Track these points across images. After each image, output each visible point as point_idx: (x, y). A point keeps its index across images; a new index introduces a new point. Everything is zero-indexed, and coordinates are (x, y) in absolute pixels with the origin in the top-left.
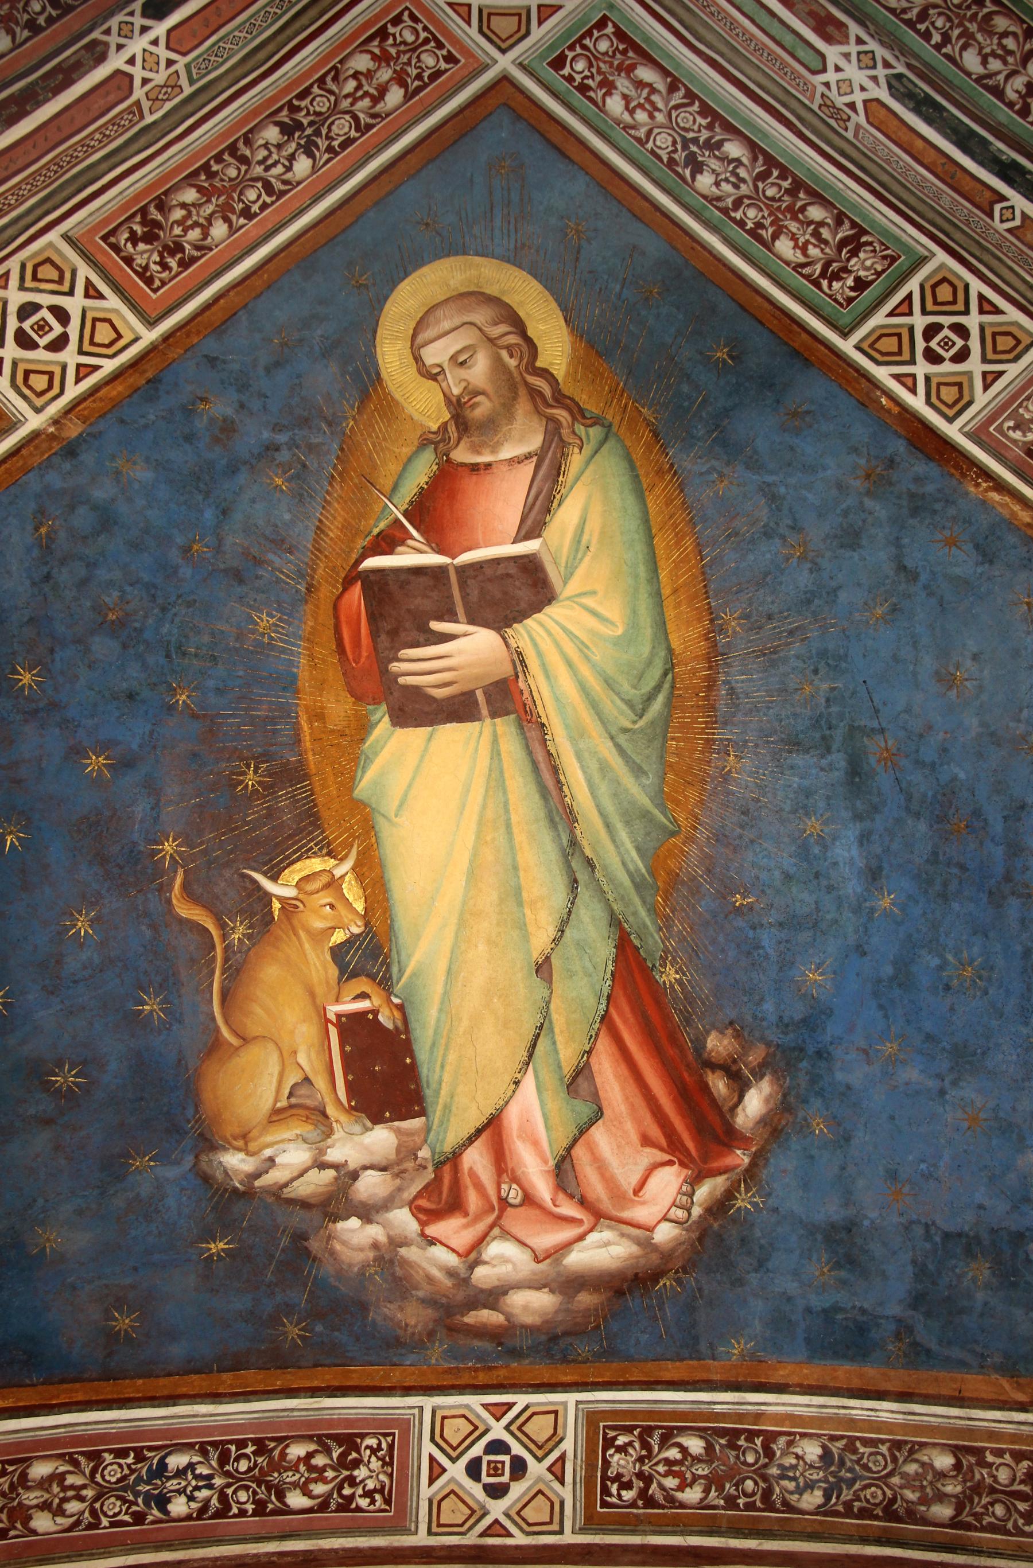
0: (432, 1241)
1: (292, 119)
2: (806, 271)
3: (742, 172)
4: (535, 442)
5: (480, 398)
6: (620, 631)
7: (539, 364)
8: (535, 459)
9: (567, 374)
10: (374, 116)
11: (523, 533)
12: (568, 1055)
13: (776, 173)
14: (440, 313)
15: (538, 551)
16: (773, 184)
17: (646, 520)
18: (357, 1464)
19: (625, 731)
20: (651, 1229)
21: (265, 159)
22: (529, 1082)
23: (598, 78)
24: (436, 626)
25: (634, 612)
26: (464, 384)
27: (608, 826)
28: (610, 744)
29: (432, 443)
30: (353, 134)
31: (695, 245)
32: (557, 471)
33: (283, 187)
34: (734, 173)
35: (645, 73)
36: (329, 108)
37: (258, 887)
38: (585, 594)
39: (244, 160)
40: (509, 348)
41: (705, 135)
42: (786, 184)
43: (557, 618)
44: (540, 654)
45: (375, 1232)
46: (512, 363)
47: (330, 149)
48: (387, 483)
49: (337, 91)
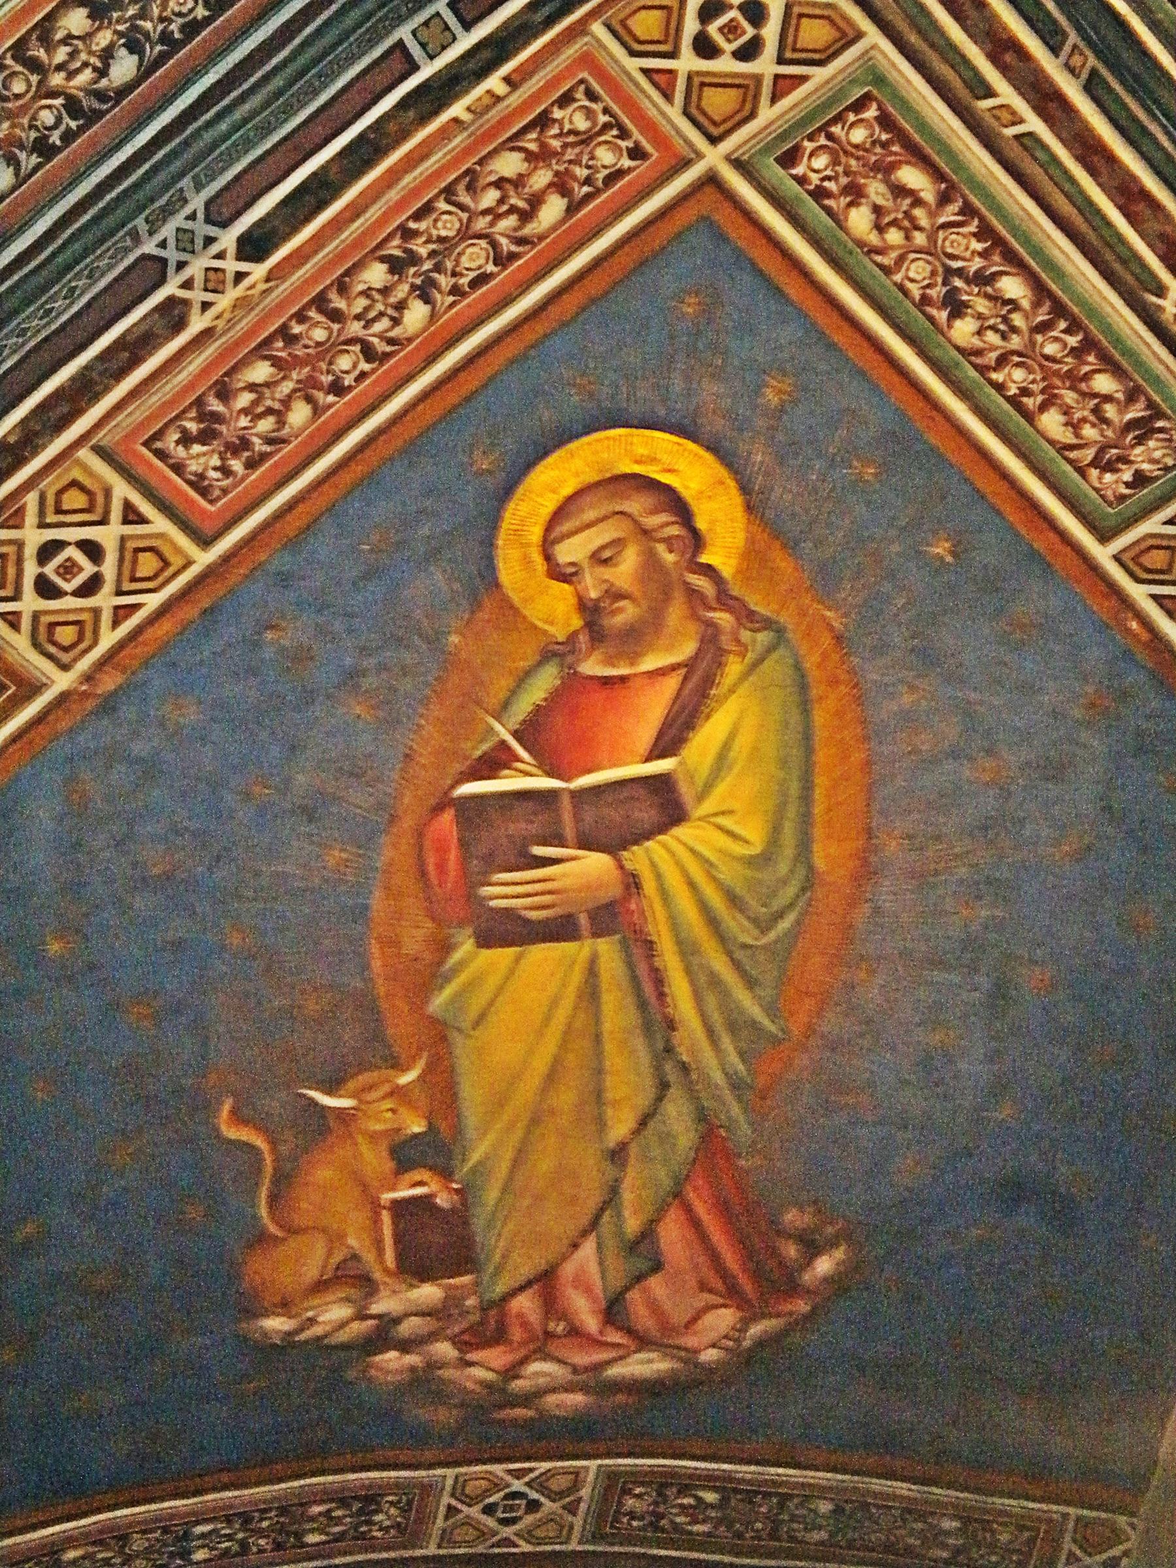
0: (471, 1364)
1: (406, 251)
2: (1073, 455)
3: (1017, 320)
4: (687, 649)
5: (622, 603)
6: (756, 849)
7: (704, 559)
8: (683, 671)
9: (739, 571)
10: (521, 241)
11: (656, 753)
12: (632, 1225)
13: (1063, 325)
14: (587, 499)
15: (675, 770)
16: (1056, 339)
17: (807, 737)
18: (377, 1512)
19: (745, 946)
20: (696, 1352)
21: (367, 309)
22: (588, 1248)
23: (844, 181)
24: (539, 851)
25: (776, 830)
26: (605, 586)
27: (710, 1032)
28: (724, 958)
29: (560, 655)
30: (490, 268)
31: (934, 413)
32: (709, 681)
33: (389, 349)
34: (1005, 320)
35: (911, 177)
36: (459, 231)
37: (313, 1103)
38: (723, 813)
39: (336, 316)
40: (668, 541)
41: (977, 263)
42: (1073, 341)
43: (682, 838)
44: (659, 877)
45: (412, 1359)
46: (669, 558)
47: (455, 290)
48: (494, 700)
49: (472, 205)
